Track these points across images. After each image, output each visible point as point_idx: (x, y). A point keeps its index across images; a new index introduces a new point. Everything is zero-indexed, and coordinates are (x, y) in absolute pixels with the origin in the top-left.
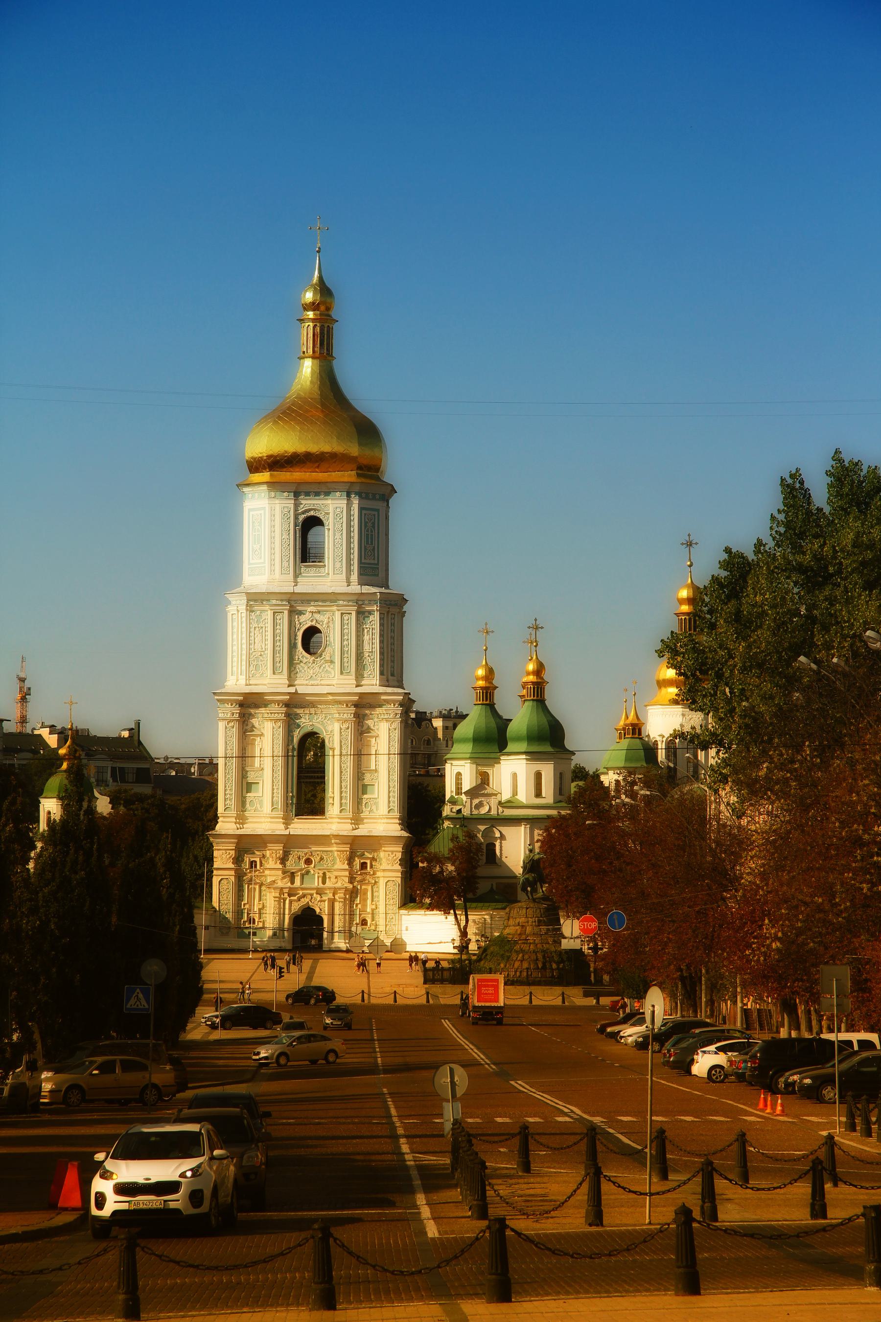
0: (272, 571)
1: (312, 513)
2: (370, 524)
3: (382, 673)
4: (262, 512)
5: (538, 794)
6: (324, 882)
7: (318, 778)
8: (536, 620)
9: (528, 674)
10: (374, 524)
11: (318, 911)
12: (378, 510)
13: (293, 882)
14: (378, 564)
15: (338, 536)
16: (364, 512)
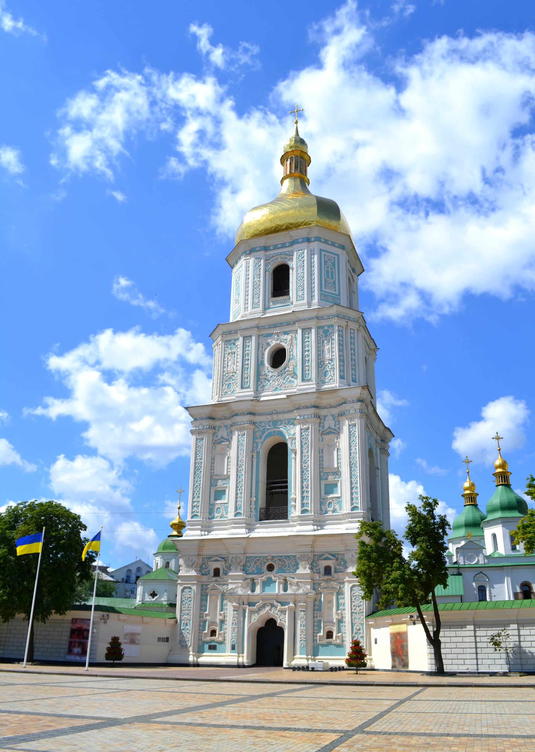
0: (246, 308)
1: (279, 259)
2: (329, 263)
3: (342, 377)
4: (241, 269)
5: (514, 548)
6: (285, 590)
7: (282, 482)
8: (497, 433)
9: (497, 467)
10: (333, 264)
11: (278, 621)
12: (338, 256)
13: (253, 590)
14: (339, 295)
15: (300, 271)
16: (323, 253)
